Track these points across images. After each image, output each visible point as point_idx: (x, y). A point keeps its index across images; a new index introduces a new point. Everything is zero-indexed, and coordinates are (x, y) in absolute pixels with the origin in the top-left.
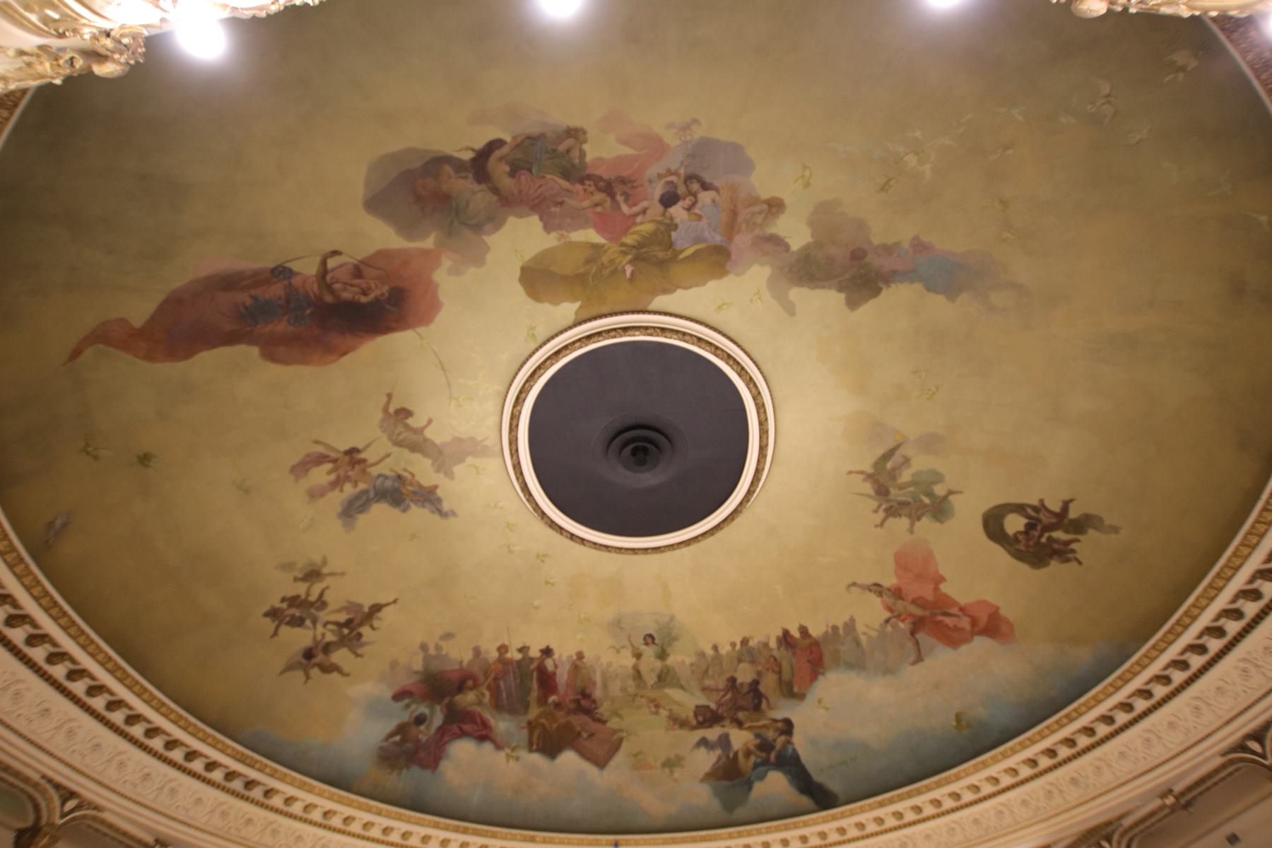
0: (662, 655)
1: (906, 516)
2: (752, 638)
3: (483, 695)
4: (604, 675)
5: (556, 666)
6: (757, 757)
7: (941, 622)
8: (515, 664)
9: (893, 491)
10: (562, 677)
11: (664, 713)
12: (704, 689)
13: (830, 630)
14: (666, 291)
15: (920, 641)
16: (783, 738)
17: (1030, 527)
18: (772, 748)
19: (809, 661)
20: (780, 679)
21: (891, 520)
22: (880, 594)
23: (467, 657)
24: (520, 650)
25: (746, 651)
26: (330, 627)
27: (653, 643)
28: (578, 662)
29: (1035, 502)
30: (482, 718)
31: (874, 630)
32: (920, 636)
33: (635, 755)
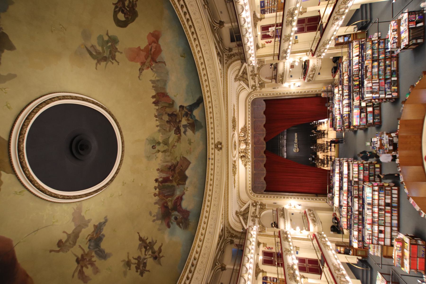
0: (159, 143)
1: (115, 53)
2: (155, 114)
3: (169, 200)
4: (164, 162)
5: (161, 177)
6: (189, 117)
7: (153, 52)
8: (160, 191)
9: (105, 55)
10: (164, 175)
11: (176, 144)
12: (170, 131)
13: (154, 88)
15: (159, 61)
16: (184, 109)
17: (123, 12)
18: (187, 112)
19: (163, 97)
20: (168, 107)
21: (116, 58)
22: (143, 69)
23: (157, 206)
24: (156, 189)
25: (159, 116)
27: (155, 146)
28: (160, 170)
29: (114, 7)
30: (176, 200)
31: (154, 75)
32: (157, 61)
33: (187, 153)
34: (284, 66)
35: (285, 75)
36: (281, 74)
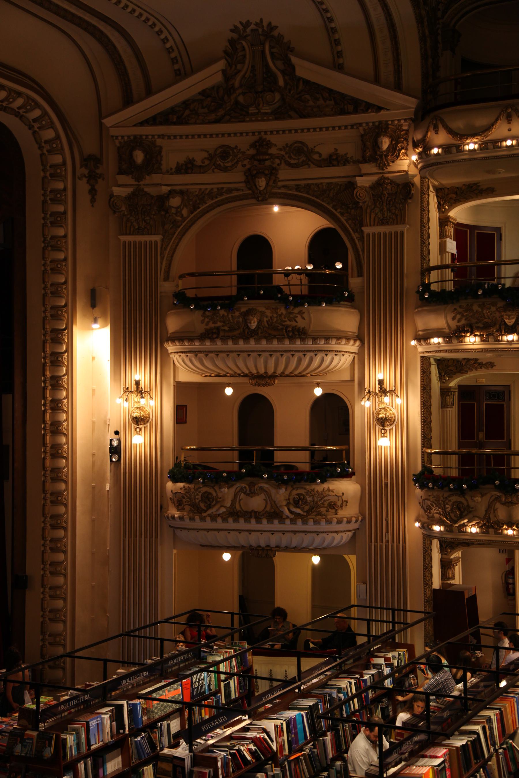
34: (348, 339)
35: (287, 344)
36: (300, 323)
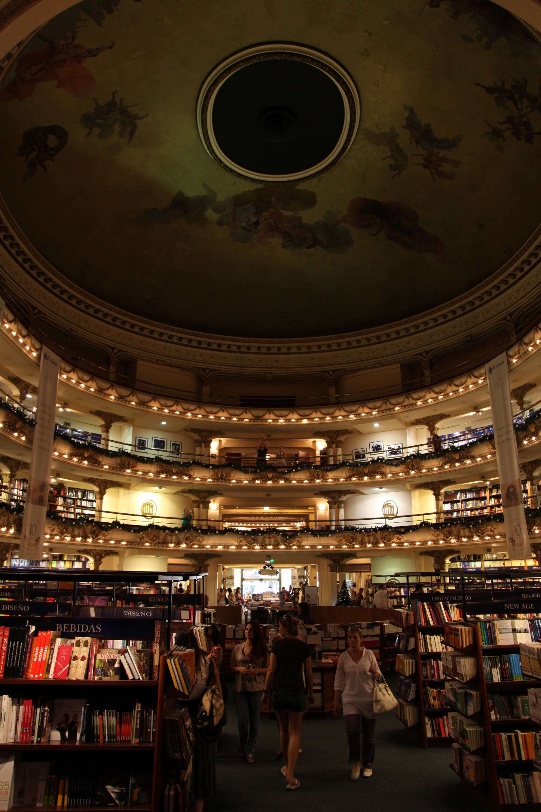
14: (258, 190)
26: (520, 107)
